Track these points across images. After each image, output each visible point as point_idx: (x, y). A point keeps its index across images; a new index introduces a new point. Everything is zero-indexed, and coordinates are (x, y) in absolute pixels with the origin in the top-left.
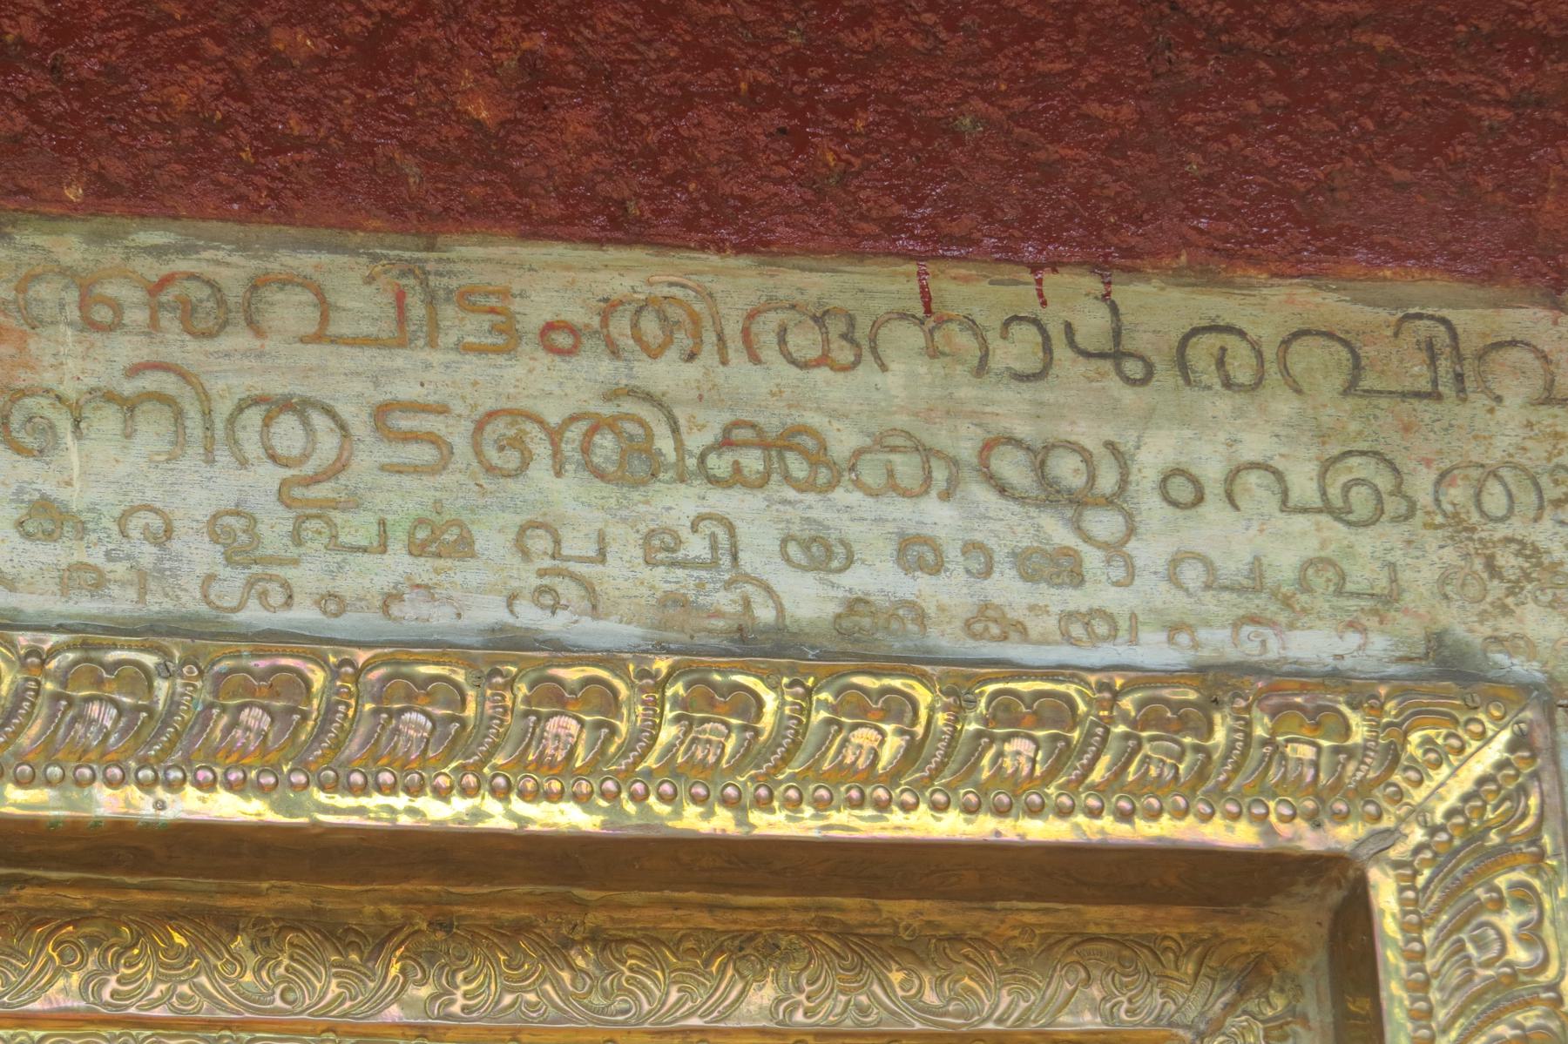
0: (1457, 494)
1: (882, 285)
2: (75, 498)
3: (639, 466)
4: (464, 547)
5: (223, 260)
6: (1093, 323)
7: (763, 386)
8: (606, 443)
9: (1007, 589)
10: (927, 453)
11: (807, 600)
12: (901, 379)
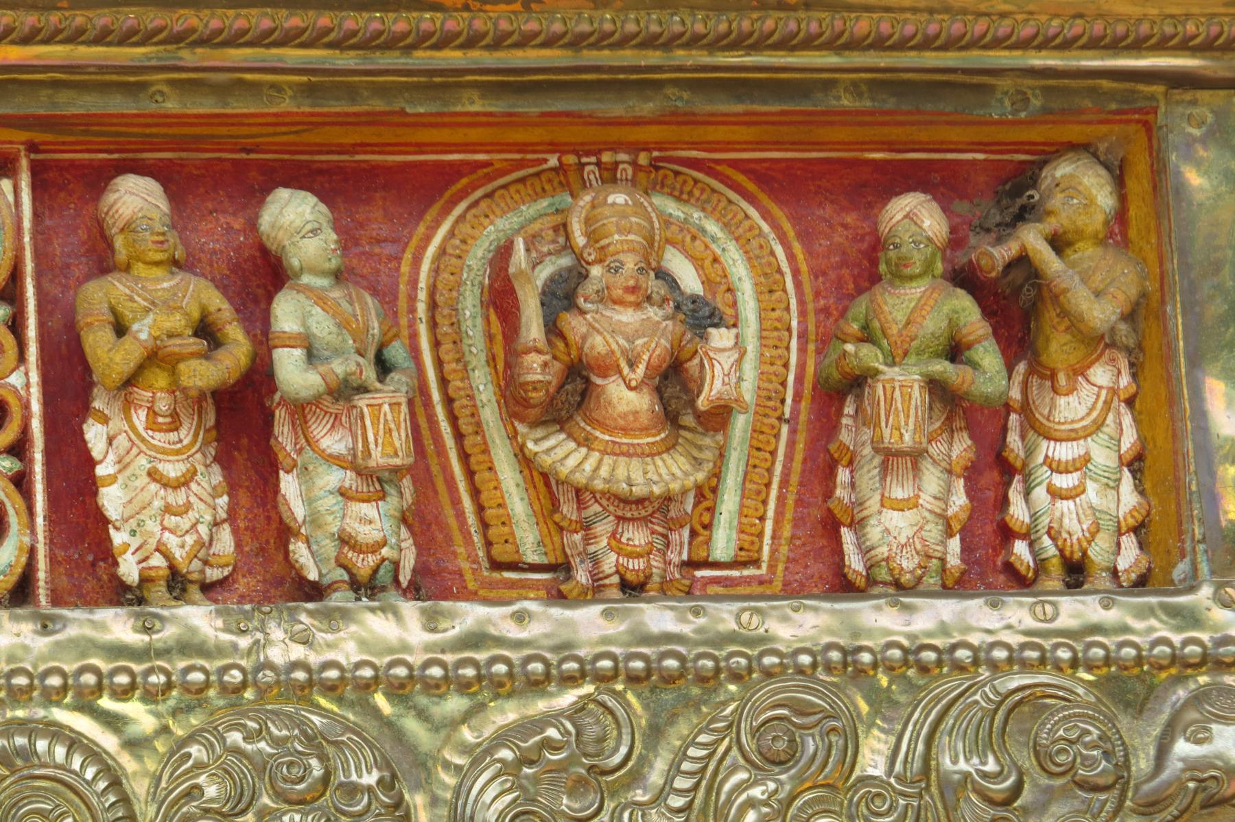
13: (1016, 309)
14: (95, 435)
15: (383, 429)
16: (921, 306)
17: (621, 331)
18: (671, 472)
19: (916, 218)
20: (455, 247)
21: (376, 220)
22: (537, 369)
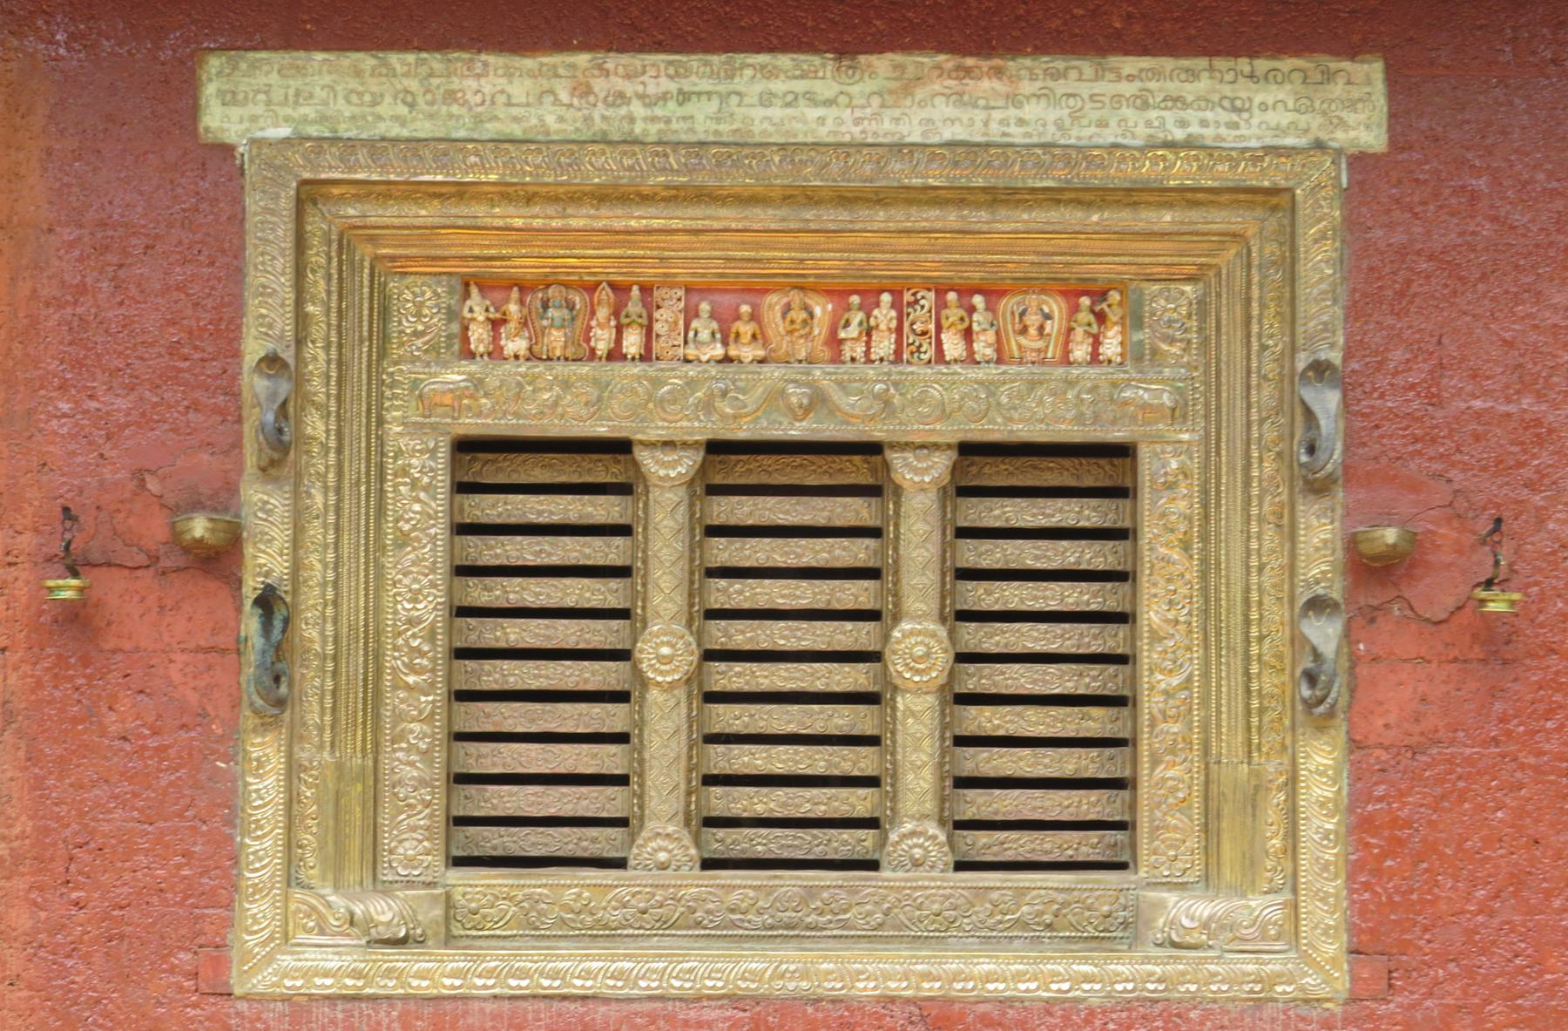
0: (1325, 106)
1: (1201, 63)
2: (1027, 117)
3: (1146, 106)
4: (1107, 125)
5: (1060, 64)
6: (1247, 69)
7: (1173, 87)
8: (1139, 101)
9: (1223, 131)
10: (1208, 101)
11: (1179, 135)
12: (1204, 84)
13: (1101, 318)
14: (943, 336)
15: (990, 336)
16: (1084, 316)
17: (1033, 320)
18: (1040, 344)
19: (1085, 301)
20: (1008, 304)
21: (993, 298)
22: (1017, 327)
